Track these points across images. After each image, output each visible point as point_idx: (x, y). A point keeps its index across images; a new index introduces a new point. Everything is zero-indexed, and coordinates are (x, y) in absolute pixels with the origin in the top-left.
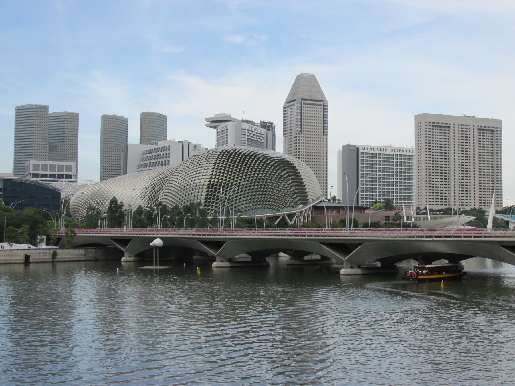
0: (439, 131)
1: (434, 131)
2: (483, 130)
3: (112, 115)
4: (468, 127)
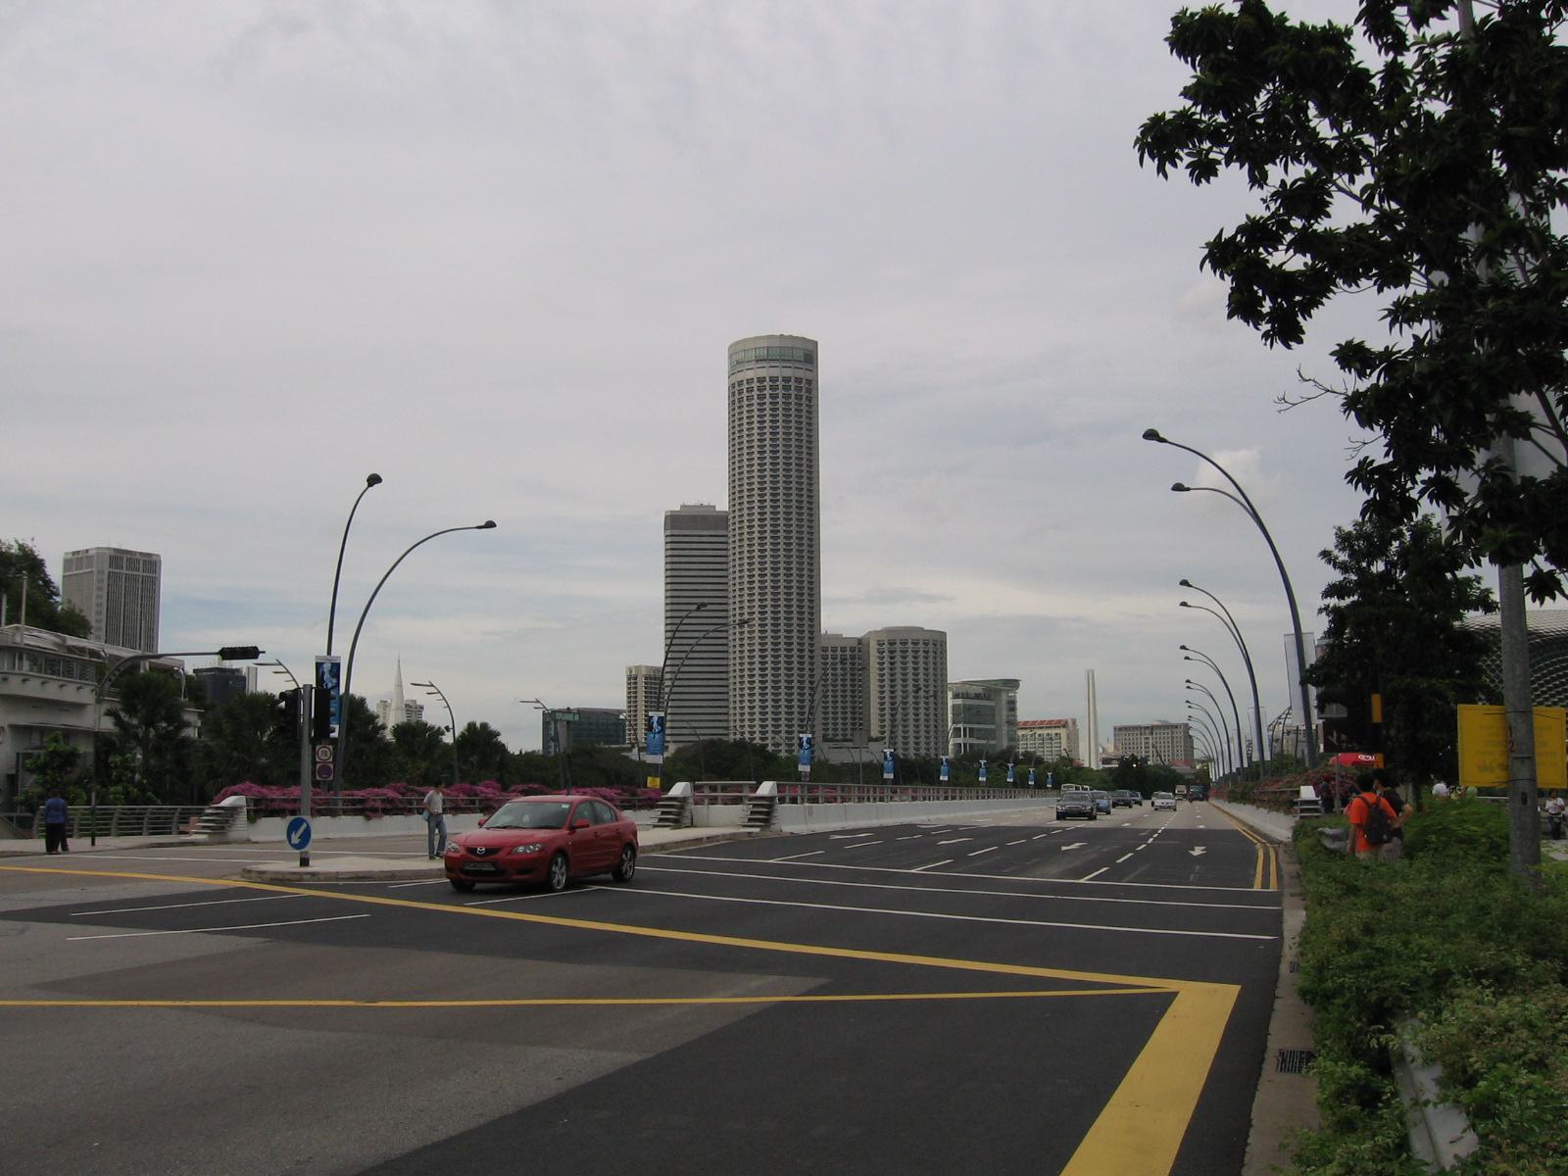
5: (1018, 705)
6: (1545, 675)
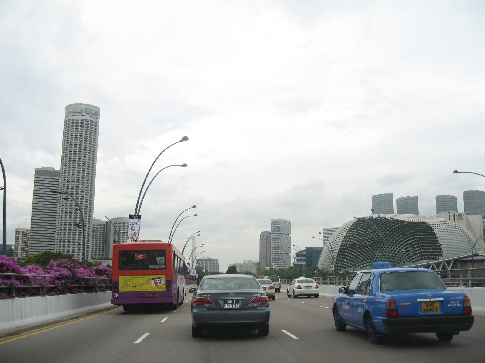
3: (443, 195)
6: (406, 238)
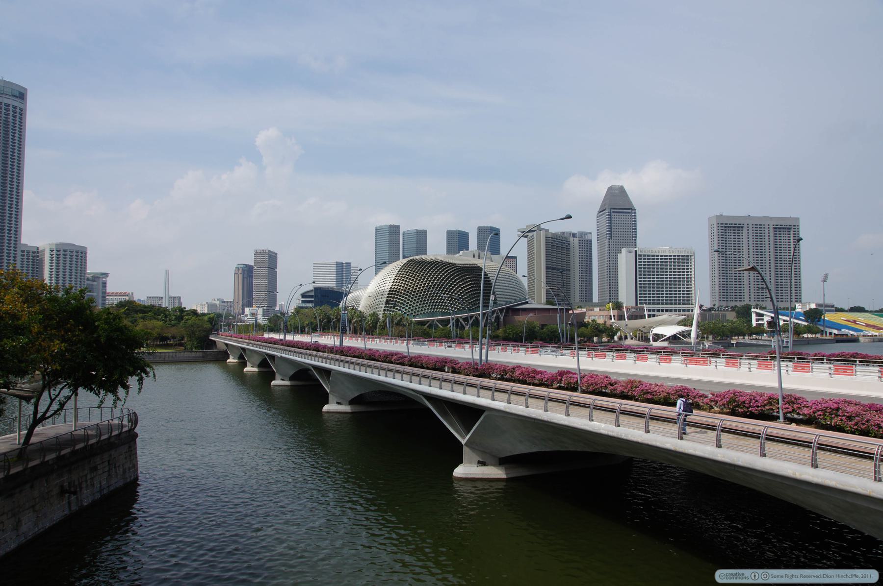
0: (732, 231)
1: (727, 231)
2: (779, 228)
4: (763, 226)
5: (108, 285)
